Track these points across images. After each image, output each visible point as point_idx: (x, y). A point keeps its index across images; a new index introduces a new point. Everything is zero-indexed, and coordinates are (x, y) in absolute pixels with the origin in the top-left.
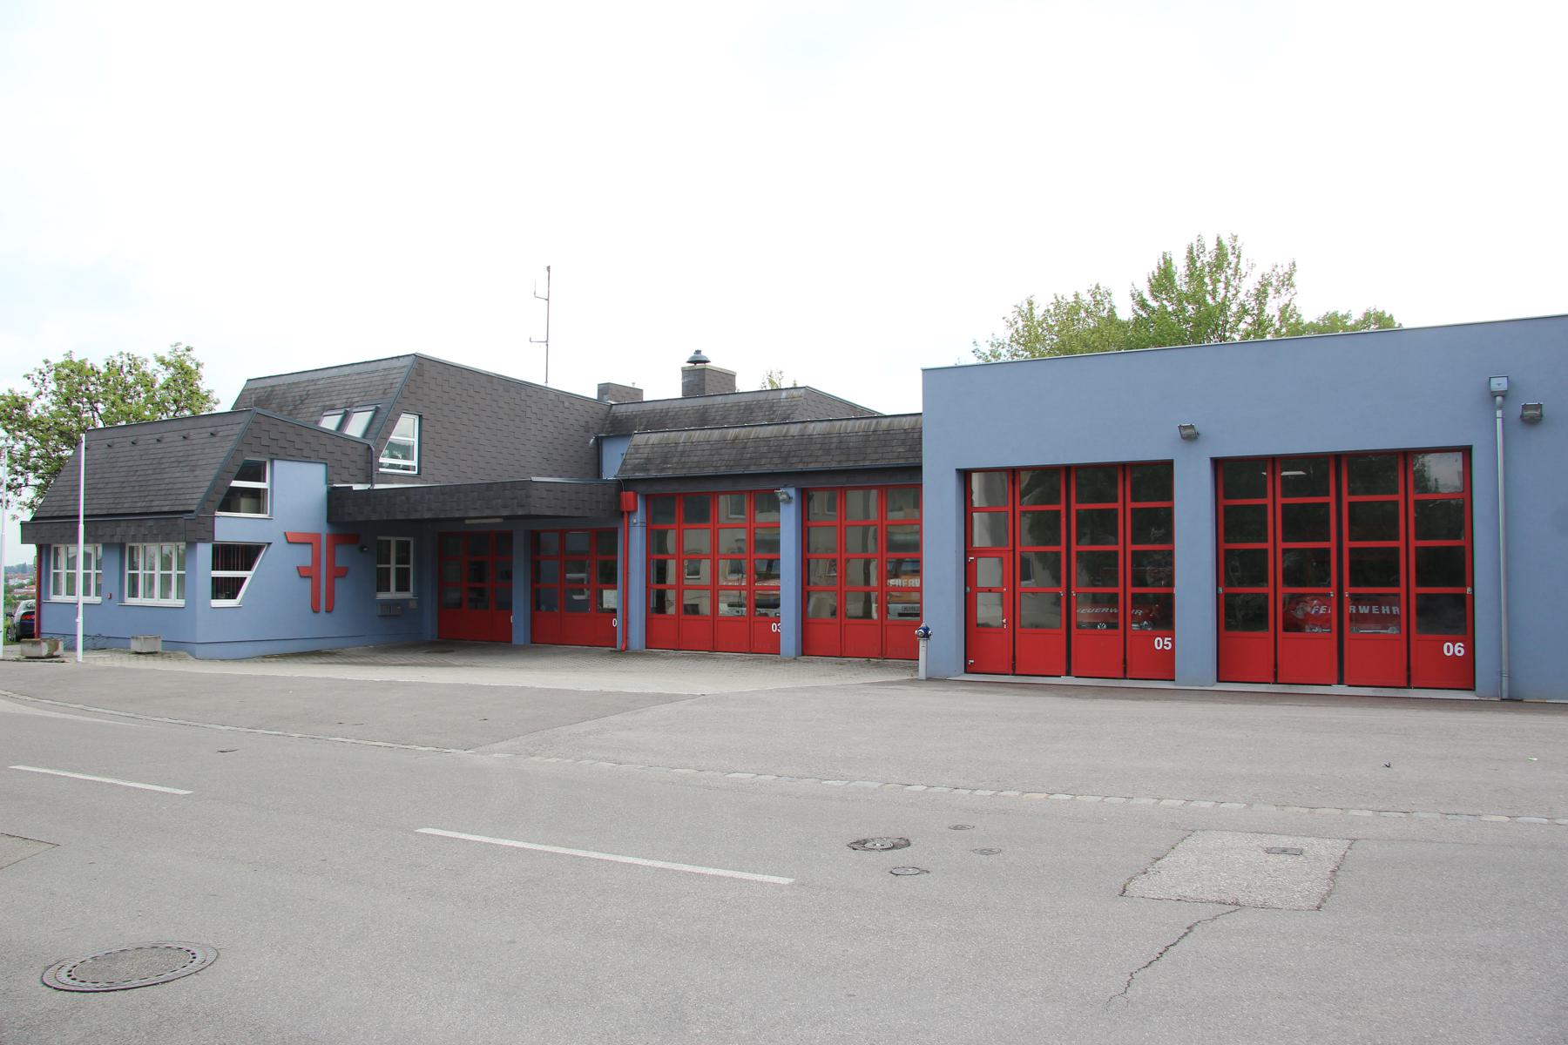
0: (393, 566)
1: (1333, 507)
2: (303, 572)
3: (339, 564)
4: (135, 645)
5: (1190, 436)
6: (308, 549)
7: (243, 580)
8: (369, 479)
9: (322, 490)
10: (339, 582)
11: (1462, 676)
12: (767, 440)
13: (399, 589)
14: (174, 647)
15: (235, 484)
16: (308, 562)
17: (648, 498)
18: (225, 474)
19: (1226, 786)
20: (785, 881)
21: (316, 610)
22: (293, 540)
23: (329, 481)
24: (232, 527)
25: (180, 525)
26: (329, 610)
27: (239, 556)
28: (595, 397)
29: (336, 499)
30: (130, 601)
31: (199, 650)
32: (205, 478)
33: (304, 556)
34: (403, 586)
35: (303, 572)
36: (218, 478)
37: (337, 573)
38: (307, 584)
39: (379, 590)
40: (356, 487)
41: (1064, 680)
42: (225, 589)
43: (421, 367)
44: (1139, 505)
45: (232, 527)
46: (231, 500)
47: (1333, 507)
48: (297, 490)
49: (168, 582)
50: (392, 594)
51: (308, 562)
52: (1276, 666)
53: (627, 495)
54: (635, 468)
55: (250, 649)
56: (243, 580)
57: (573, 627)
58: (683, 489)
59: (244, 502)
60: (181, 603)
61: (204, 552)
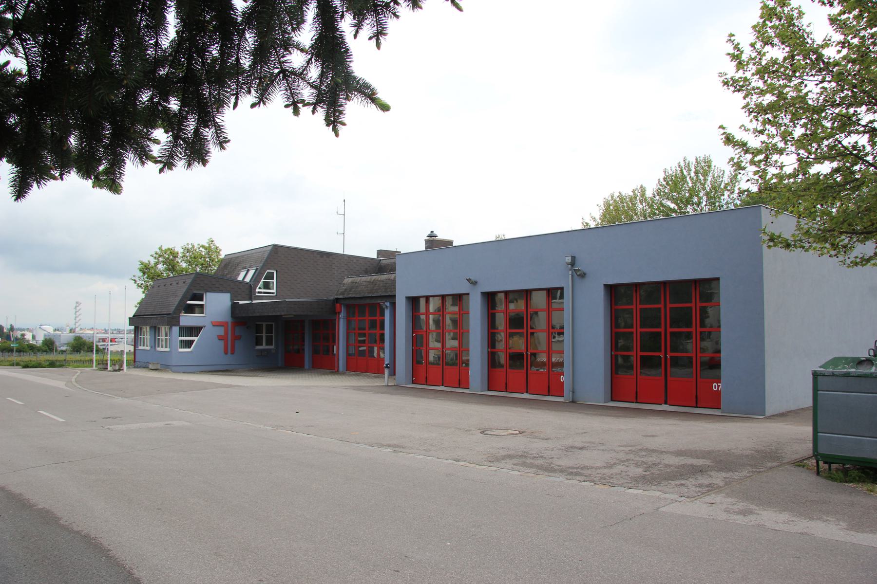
0: (264, 335)
1: (694, 308)
2: (220, 338)
3: (237, 333)
4: (151, 366)
5: (474, 283)
6: (222, 329)
7: (193, 341)
8: (250, 299)
9: (229, 303)
10: (237, 343)
11: (713, 401)
12: (383, 281)
13: (267, 345)
14: (165, 367)
15: (189, 302)
16: (222, 333)
17: (348, 307)
18: (184, 298)
19: (588, 448)
20: (42, 412)
21: (226, 353)
22: (216, 324)
23: (232, 300)
24: (187, 319)
25: (172, 320)
26: (233, 353)
27: (194, 331)
28: (375, 257)
29: (234, 307)
30: (158, 349)
31: (173, 368)
32: (175, 301)
33: (221, 331)
34: (269, 342)
35: (220, 338)
36: (181, 300)
37: (235, 338)
38: (222, 342)
39: (257, 344)
40: (241, 302)
41: (442, 388)
42: (189, 344)
43: (276, 249)
44: (689, 305)
45: (187, 319)
46: (190, 309)
47: (694, 308)
48: (217, 304)
49: (170, 341)
50: (264, 346)
51: (222, 333)
52: (696, 397)
53: (338, 305)
54: (343, 293)
55: (196, 369)
56: (193, 341)
57: (323, 362)
58: (357, 302)
59: (197, 309)
60: (168, 350)
61: (176, 329)
